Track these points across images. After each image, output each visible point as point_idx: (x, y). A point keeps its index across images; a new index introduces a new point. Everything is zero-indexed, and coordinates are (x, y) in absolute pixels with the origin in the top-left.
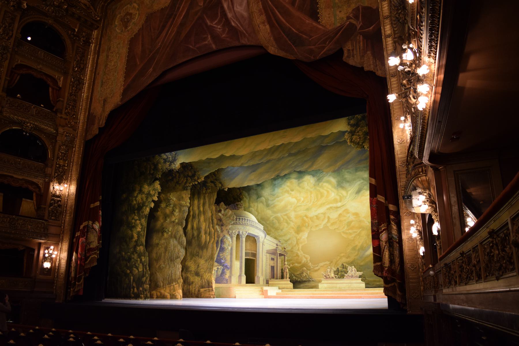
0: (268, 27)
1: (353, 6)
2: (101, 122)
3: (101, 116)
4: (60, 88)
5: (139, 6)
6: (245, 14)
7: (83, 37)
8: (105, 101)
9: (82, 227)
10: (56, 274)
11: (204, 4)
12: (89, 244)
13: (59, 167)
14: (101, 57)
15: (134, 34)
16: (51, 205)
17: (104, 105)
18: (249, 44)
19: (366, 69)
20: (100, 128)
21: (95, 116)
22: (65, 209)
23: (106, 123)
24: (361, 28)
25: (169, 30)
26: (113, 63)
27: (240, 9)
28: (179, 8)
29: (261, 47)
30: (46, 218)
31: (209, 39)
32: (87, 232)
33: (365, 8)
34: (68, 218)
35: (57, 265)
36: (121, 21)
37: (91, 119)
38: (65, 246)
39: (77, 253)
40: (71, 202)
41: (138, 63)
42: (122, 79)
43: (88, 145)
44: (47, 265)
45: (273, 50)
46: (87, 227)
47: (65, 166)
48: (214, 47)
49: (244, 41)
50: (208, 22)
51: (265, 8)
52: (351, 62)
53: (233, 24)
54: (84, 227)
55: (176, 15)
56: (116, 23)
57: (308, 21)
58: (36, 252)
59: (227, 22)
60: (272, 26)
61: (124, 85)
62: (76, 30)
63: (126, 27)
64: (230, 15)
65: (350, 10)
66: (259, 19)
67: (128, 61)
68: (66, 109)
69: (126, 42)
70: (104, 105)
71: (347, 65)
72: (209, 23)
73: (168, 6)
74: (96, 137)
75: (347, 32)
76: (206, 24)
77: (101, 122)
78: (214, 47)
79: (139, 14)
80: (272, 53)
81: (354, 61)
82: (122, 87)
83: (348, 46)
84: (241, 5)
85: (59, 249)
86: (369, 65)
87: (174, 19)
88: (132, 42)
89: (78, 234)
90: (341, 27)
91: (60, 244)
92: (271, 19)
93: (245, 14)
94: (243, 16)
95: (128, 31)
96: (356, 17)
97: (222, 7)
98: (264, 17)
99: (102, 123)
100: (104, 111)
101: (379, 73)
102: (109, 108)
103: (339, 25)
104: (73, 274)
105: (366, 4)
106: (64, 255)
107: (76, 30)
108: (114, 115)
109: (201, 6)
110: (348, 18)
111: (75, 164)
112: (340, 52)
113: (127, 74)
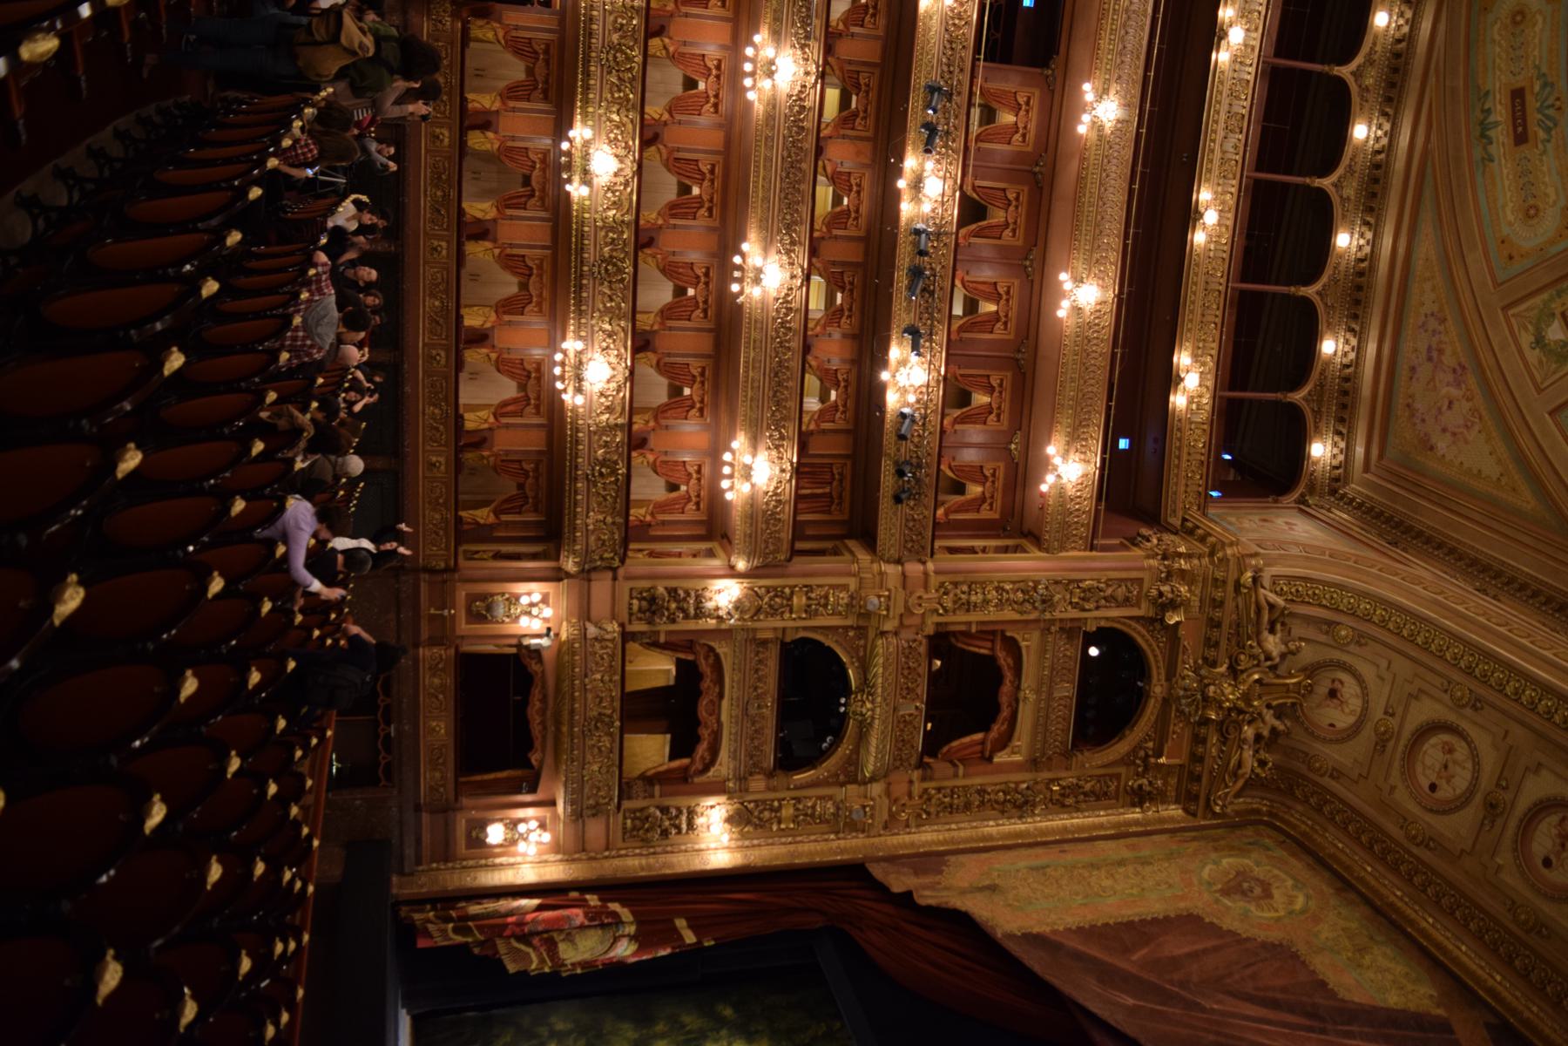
3: (946, 888)
4: (990, 759)
5: (1303, 911)
7: (1150, 783)
8: (993, 888)
9: (614, 906)
10: (471, 863)
12: (569, 938)
13: (772, 809)
14: (1111, 844)
16: (665, 810)
17: (981, 889)
21: (940, 872)
22: (659, 849)
23: (929, 907)
25: (1269, 1022)
26: (1107, 883)
30: (626, 804)
32: (602, 926)
34: (634, 864)
35: (498, 861)
36: (1238, 873)
37: (930, 861)
38: (555, 872)
39: (539, 908)
41: (1135, 958)
42: (1072, 921)
43: (855, 873)
44: (495, 833)
46: (618, 921)
47: (779, 822)
54: (615, 914)
55: (1323, 1031)
56: (1225, 861)
58: (528, 798)
61: (1055, 932)
62: (1162, 760)
63: (1226, 892)
68: (939, 790)
69: (1182, 905)
70: (981, 889)
73: (1343, 1000)
74: (882, 890)
77: (927, 893)
79: (1278, 919)
85: (545, 857)
87: (1311, 1029)
88: (1190, 923)
89: (593, 900)
91: (559, 857)
95: (1217, 901)
99: (926, 898)
100: (962, 892)
104: (474, 909)
106: (528, 875)
107: (1162, 760)
108: (960, 922)
111: (792, 848)
113: (1089, 933)
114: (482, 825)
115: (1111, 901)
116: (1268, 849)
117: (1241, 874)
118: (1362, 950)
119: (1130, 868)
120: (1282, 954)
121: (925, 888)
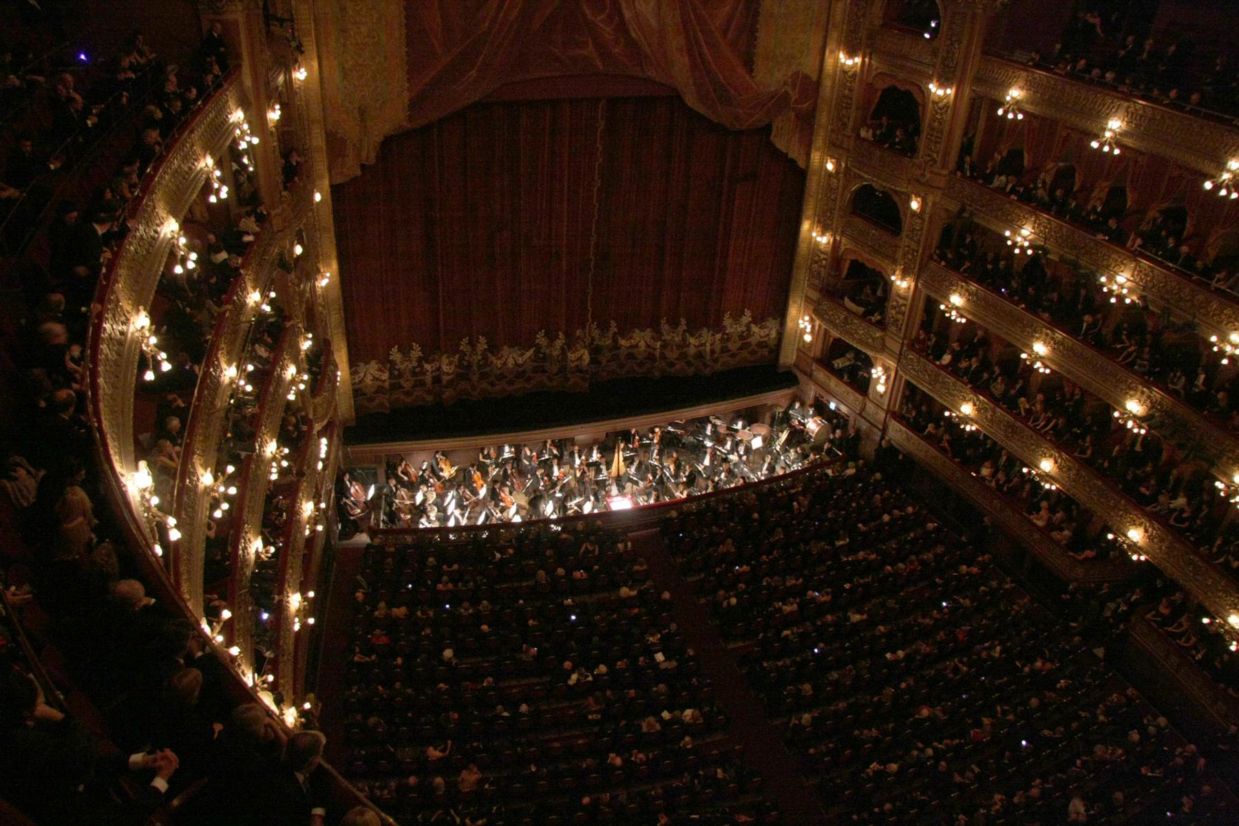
1: (794, 68)
2: (364, 154)
3: (361, 140)
6: (653, 22)
8: (362, 112)
17: (363, 120)
19: (790, 156)
20: (363, 166)
27: (646, 9)
29: (675, 90)
33: (806, 77)
37: (336, 145)
40: (336, 293)
45: (691, 100)
50: (588, 12)
52: (778, 146)
53: (634, 35)
57: (741, 70)
59: (622, 27)
64: (627, 14)
66: (675, 42)
71: (773, 145)
72: (590, 17)
75: (780, 102)
77: (364, 154)
81: (780, 144)
82: (406, 94)
86: (795, 153)
93: (653, 22)
99: (370, 155)
101: (801, 164)
102: (380, 129)
103: (773, 89)
110: (785, 84)
112: (767, 129)
113: (414, 67)
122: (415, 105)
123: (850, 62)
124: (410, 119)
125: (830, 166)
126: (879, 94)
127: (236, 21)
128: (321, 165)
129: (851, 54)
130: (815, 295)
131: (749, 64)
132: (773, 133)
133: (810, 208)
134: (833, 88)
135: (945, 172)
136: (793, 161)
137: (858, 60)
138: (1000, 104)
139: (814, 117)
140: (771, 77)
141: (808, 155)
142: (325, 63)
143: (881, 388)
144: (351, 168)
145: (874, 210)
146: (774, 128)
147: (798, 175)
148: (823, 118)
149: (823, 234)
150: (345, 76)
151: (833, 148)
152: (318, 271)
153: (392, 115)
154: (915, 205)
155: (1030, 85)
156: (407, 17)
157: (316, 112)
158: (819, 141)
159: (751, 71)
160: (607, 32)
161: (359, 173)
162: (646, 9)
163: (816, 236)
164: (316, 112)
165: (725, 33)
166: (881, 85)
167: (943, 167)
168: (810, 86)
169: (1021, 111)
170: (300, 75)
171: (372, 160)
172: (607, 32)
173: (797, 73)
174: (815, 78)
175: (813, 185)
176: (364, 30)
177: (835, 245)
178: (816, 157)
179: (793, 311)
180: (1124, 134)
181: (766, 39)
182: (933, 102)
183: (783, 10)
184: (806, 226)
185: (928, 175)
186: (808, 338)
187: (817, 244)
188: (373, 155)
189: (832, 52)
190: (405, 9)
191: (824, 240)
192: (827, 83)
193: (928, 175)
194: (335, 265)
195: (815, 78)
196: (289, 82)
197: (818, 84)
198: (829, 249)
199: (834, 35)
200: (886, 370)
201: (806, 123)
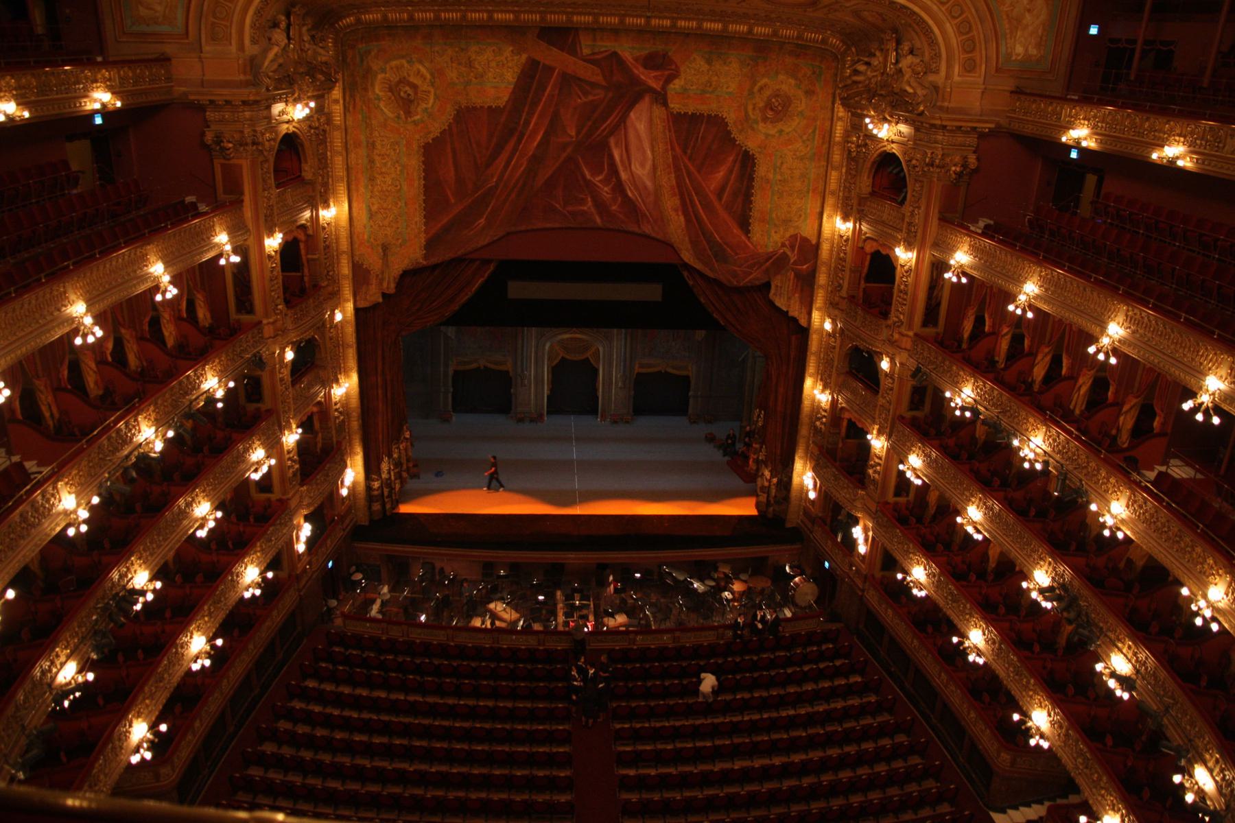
0: (682, 219)
1: (791, 232)
2: (385, 285)
3: (383, 273)
5: (432, 74)
6: (649, 184)
8: (385, 248)
11: (578, 133)
14: (353, 156)
15: (432, 136)
18: (653, 235)
19: (791, 314)
20: (384, 295)
21: (368, 271)
24: (795, 263)
28: (527, 123)
31: (590, 204)
33: (805, 240)
34: (355, 424)
36: (391, 90)
37: (360, 276)
40: (355, 402)
42: (418, 218)
45: (687, 256)
48: (598, 220)
49: (647, 229)
51: (679, 185)
52: (778, 304)
53: (630, 194)
55: (522, 135)
56: (377, 91)
57: (736, 230)
59: (619, 188)
60: (688, 221)
63: (408, 113)
64: (624, 176)
65: (788, 235)
66: (670, 203)
67: (428, 189)
69: (415, 147)
72: (588, 177)
74: (375, 306)
75: (778, 262)
76: (584, 177)
77: (385, 285)
78: (598, 220)
80: (686, 260)
81: (780, 303)
82: (423, 235)
83: (776, 282)
84: (643, 165)
86: (795, 311)
87: (519, 141)
88: (431, 152)
90: (774, 253)
92: (686, 208)
93: (649, 184)
94: (646, 188)
96: (792, 247)
97: (611, 157)
98: (676, 201)
101: (803, 322)
102: (399, 264)
105: (805, 234)
109: (571, 137)
110: (783, 245)
112: (767, 286)
114: (343, 498)
115: (405, 188)
116: (369, 52)
117: (392, 89)
118: (470, 64)
119: (377, 158)
120: (465, 115)
121: (381, 283)
122: (430, 245)
123: (840, 226)
124: (426, 257)
125: (828, 326)
126: (869, 257)
127: (240, 167)
128: (347, 292)
129: (845, 218)
130: (816, 452)
131: (744, 224)
132: (773, 291)
133: (811, 367)
134: (831, 250)
135: (911, 334)
136: (795, 320)
137: (850, 225)
138: (947, 267)
139: (814, 277)
140: (767, 238)
141: (810, 314)
142: (355, 205)
143: (862, 549)
144: (373, 296)
145: (856, 368)
146: (773, 287)
147: (804, 332)
148: (822, 279)
149: (823, 391)
150: (371, 215)
151: (832, 308)
152: (337, 381)
153: (411, 253)
154: (885, 365)
155: (975, 250)
156: (424, 171)
157: (344, 245)
158: (819, 300)
159: (749, 231)
160: (606, 191)
161: (381, 300)
162: (641, 171)
163: (817, 394)
164: (344, 245)
165: (720, 199)
166: (870, 248)
167: (910, 328)
168: (809, 249)
169: (965, 274)
170: (328, 214)
171: (392, 290)
172: (606, 191)
173: (794, 237)
174: (814, 242)
175: (814, 343)
176: (389, 180)
177: (834, 403)
178: (816, 315)
179: (798, 465)
180: (1037, 297)
181: (761, 202)
182: (902, 266)
183: (778, 177)
184: (808, 382)
185: (896, 336)
186: (812, 495)
187: (819, 402)
188: (393, 285)
189: (830, 217)
190: (423, 162)
191: (824, 398)
192: (825, 247)
193: (896, 336)
194: (354, 378)
195: (814, 242)
196: (315, 220)
197: (817, 247)
198: (827, 407)
199: (830, 201)
200: (866, 530)
201: (806, 283)
